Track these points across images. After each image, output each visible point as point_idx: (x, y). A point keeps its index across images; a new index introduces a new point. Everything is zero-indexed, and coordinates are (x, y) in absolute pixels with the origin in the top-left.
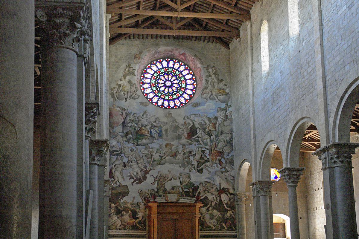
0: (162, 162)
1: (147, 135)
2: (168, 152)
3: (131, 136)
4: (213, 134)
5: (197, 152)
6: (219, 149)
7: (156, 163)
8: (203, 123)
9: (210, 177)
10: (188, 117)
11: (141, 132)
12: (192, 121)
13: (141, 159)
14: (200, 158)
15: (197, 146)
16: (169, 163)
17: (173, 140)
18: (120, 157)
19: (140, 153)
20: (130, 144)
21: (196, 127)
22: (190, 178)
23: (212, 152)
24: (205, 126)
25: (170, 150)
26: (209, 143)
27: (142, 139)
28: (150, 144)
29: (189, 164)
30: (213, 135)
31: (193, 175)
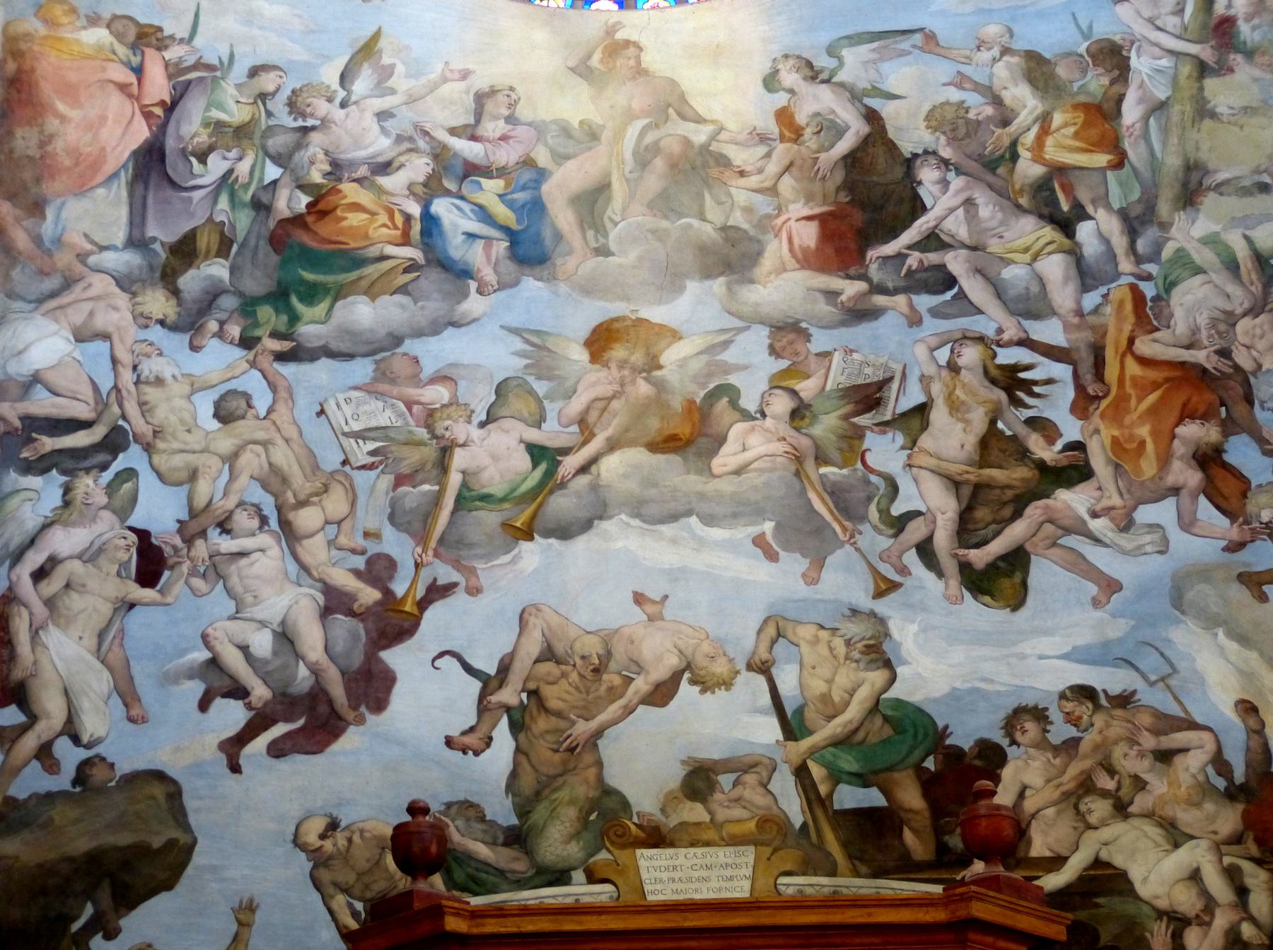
0: (561, 504)
1: (390, 250)
2: (616, 404)
3: (218, 270)
4: (1103, 200)
5: (936, 388)
6: (1188, 347)
7: (489, 519)
8: (979, 107)
9: (1120, 641)
10: (809, 65)
11: (325, 228)
12: (855, 95)
13: (326, 489)
14: (984, 443)
15: (932, 326)
16: (637, 515)
17: (671, 282)
18: (107, 476)
19: (317, 433)
20: (213, 345)
21: (907, 148)
22: (888, 664)
23: (1111, 373)
24: (1003, 136)
25: (643, 388)
26: (1063, 295)
27: (340, 293)
28: (419, 333)
29: (863, 518)
30: (1101, 214)
31: (914, 628)
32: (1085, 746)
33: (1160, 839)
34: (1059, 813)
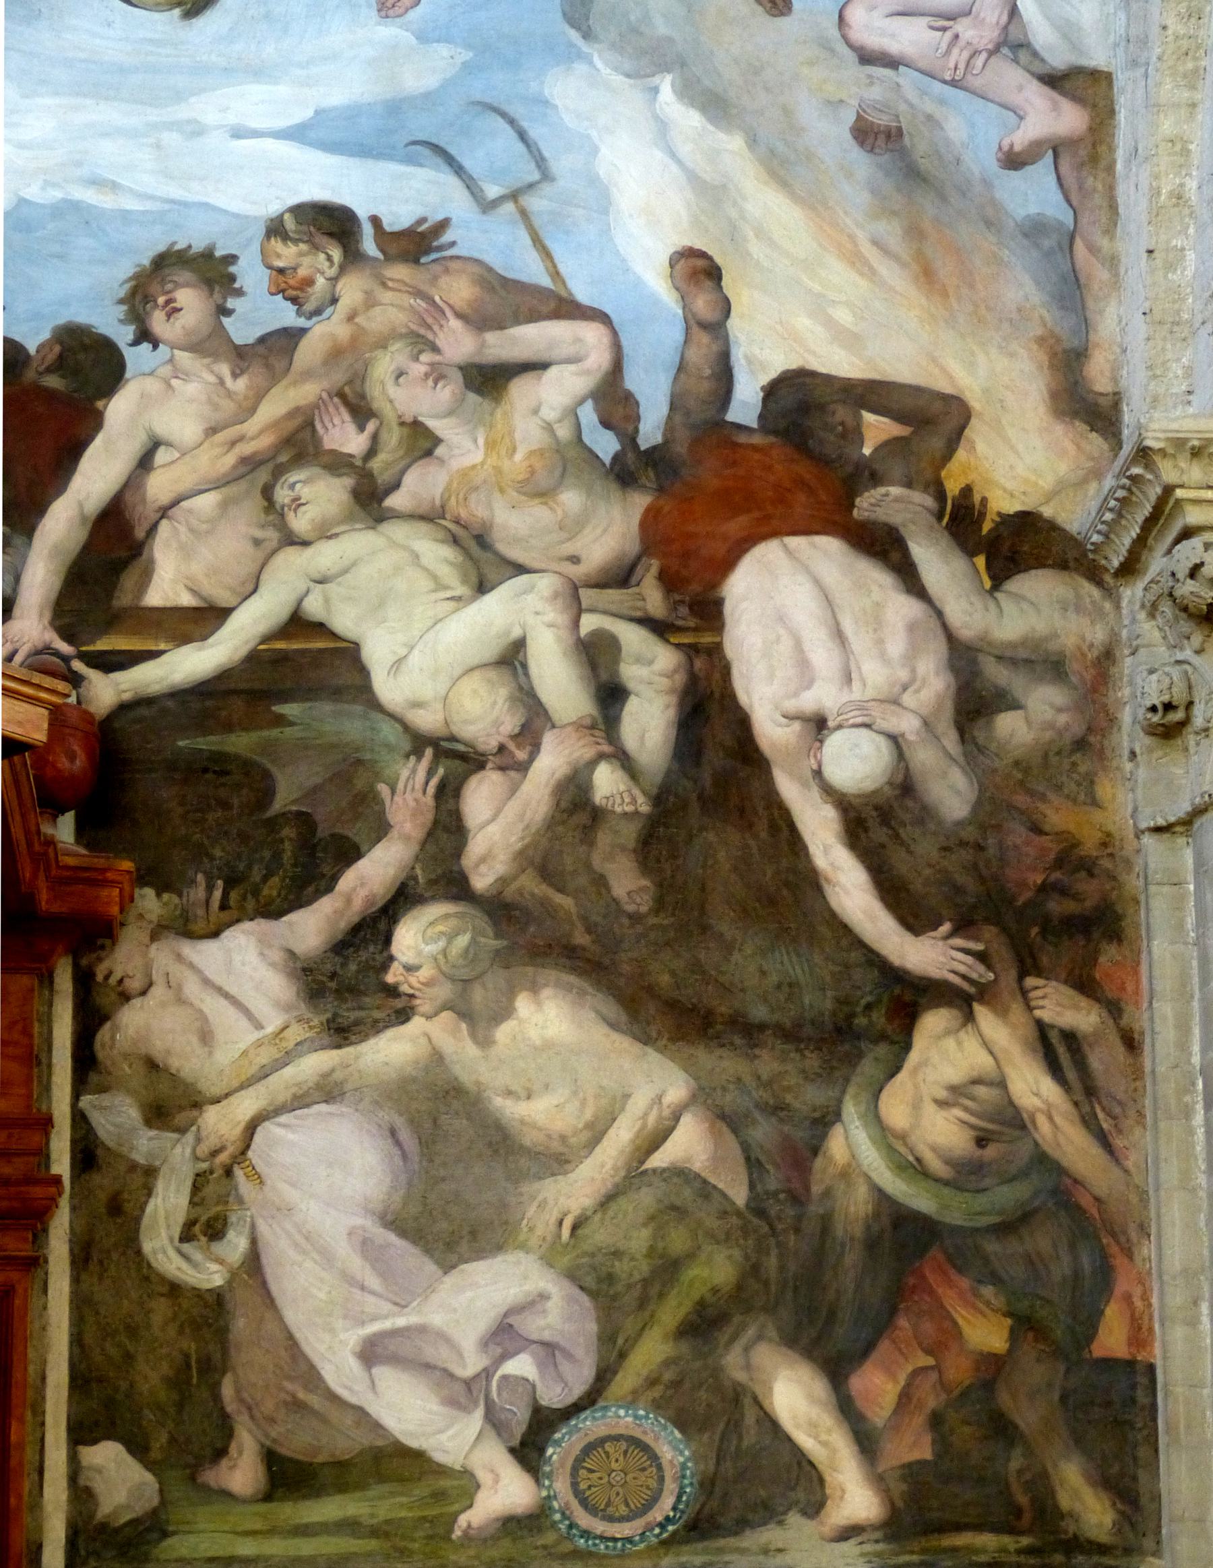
32: (309, 351)
33: (448, 574)
34: (224, 505)
